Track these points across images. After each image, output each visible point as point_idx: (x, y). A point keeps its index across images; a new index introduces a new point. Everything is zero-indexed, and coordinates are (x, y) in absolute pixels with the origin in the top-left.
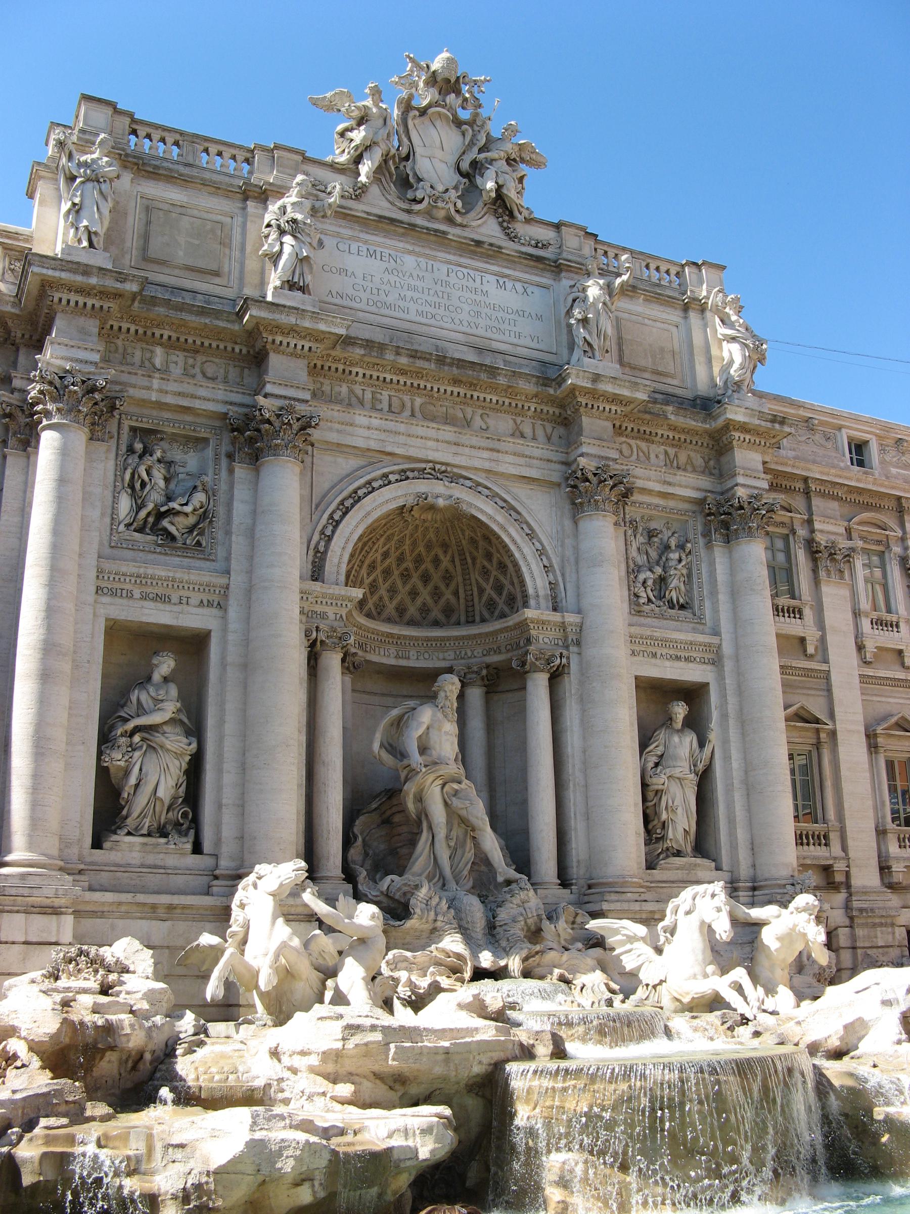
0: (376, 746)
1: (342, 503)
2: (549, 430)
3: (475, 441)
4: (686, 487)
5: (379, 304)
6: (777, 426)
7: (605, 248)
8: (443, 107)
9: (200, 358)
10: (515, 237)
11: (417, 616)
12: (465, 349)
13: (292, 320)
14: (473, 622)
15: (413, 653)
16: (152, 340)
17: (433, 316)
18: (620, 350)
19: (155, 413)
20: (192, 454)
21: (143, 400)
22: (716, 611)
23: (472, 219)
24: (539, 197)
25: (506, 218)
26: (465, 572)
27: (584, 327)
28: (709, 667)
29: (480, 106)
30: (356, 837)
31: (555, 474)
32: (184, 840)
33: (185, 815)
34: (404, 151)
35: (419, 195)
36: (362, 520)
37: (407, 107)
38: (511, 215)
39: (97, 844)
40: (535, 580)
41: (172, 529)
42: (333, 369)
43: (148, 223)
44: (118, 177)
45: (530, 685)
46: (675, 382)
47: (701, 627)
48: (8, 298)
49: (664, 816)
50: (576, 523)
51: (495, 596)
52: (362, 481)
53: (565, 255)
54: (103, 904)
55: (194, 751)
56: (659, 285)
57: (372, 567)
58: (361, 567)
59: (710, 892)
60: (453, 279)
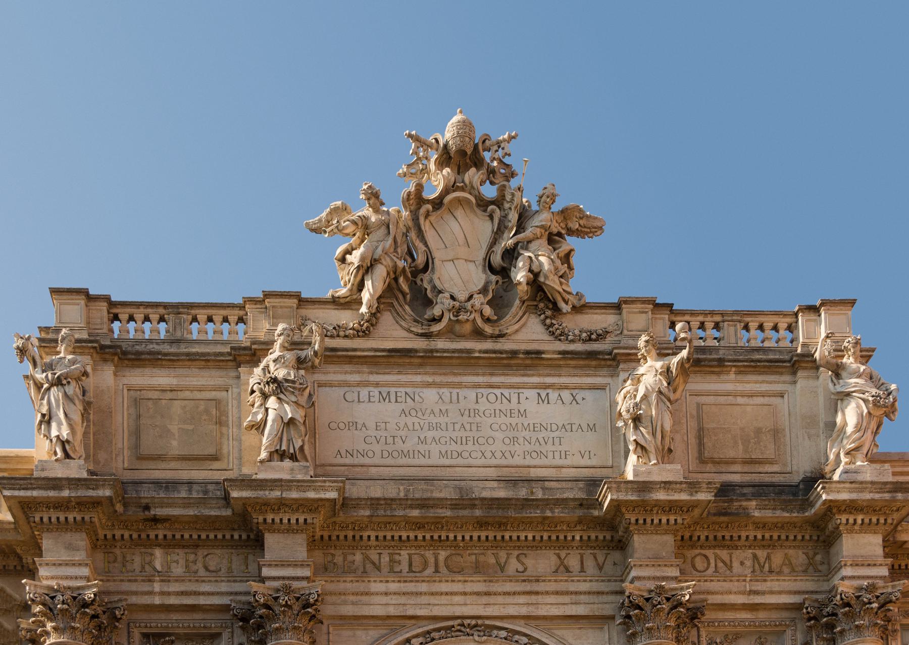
2: (601, 559)
3: (509, 587)
5: (395, 454)
9: (201, 552)
12: (495, 484)
17: (460, 455)
21: (148, 605)
23: (509, 323)
24: (594, 273)
25: (549, 313)
34: (420, 260)
38: (556, 309)
42: (342, 537)
43: (139, 417)
48: (8, 527)
60: (483, 406)
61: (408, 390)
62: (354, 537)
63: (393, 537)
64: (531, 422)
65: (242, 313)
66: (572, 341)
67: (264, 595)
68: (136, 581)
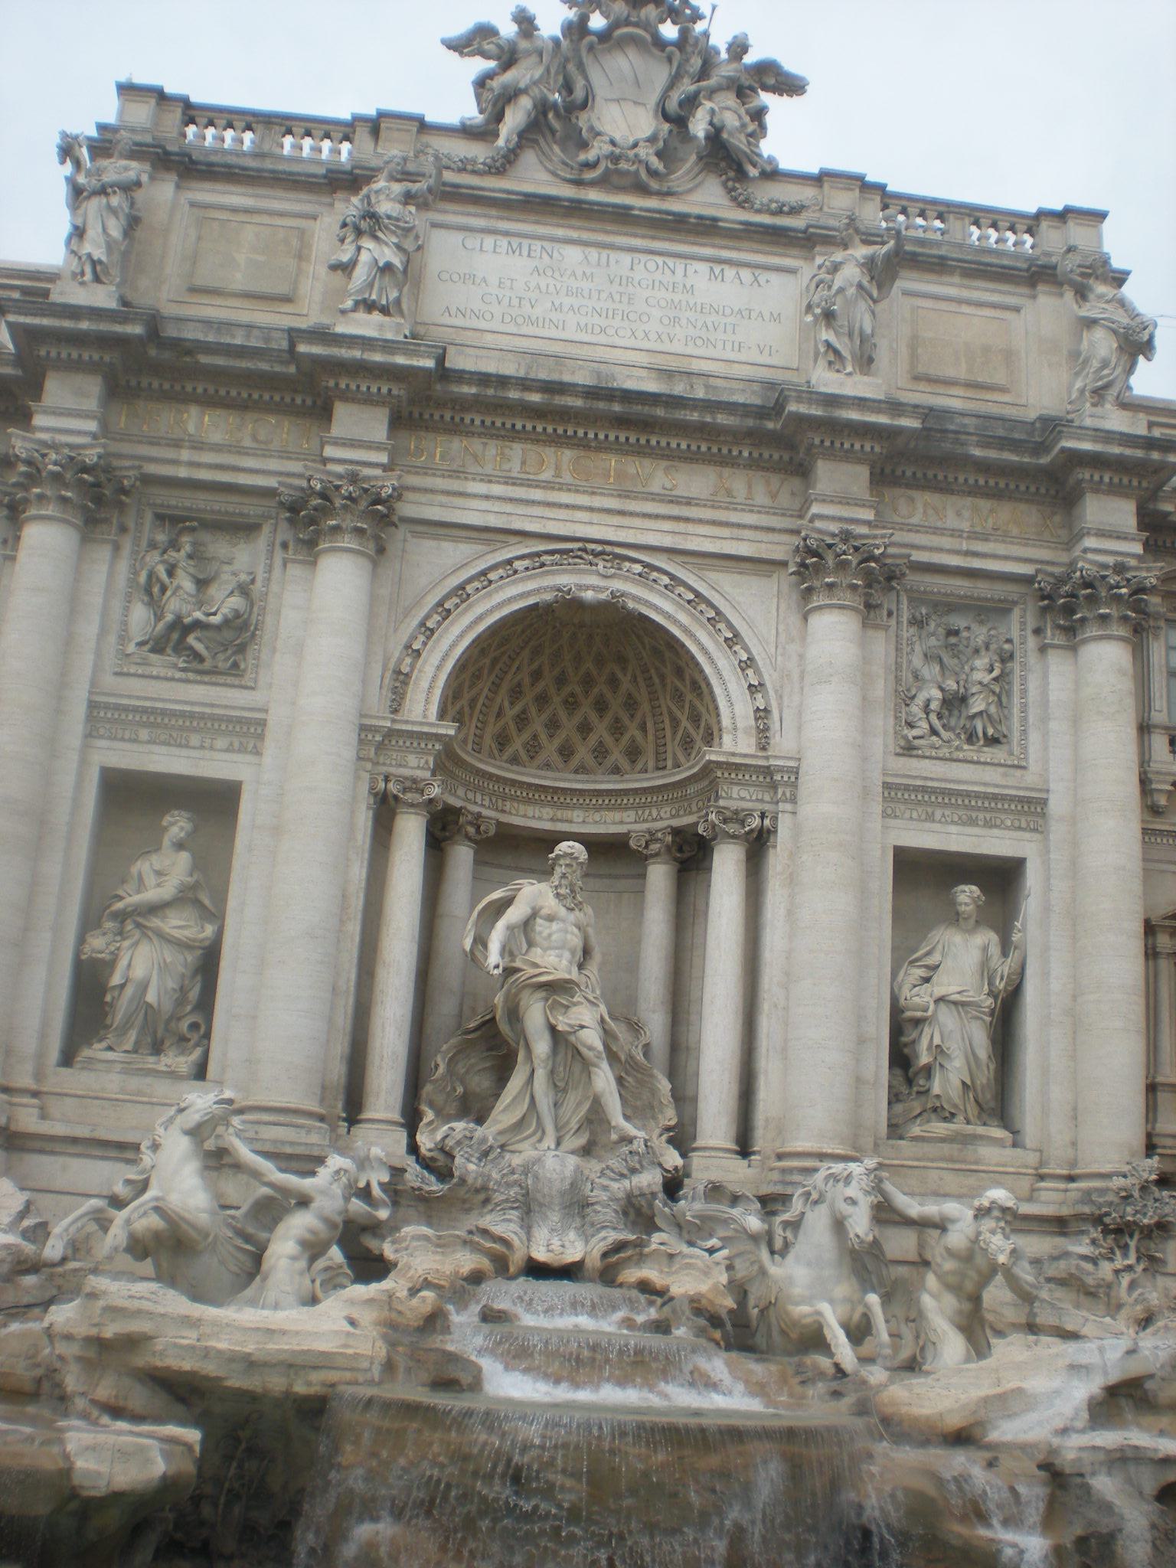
0: (468, 944)
1: (440, 604)
3: (650, 507)
4: (1006, 558)
5: (520, 320)
6: (1155, 455)
7: (904, 203)
8: (636, 25)
10: (746, 201)
11: (590, 761)
12: (644, 373)
13: (357, 354)
14: (665, 768)
15: (577, 815)
16: (185, 399)
17: (603, 330)
18: (914, 357)
19: (188, 494)
20: (242, 546)
22: (1046, 749)
24: (793, 138)
25: (732, 174)
26: (653, 697)
27: (829, 325)
28: (1027, 835)
29: (701, 17)
30: (437, 1066)
31: (778, 548)
32: (182, 1059)
33: (194, 1026)
35: (591, 155)
36: (470, 627)
37: (577, 29)
39: (67, 1059)
40: (733, 705)
41: (199, 647)
42: (437, 417)
43: (199, 238)
44: (138, 184)
45: (716, 857)
46: (1006, 398)
47: (1018, 773)
49: (924, 1059)
50: (805, 618)
51: (692, 731)
52: (472, 571)
53: (822, 222)
54: (53, 1138)
55: (207, 943)
56: (990, 252)
57: (516, 693)
58: (495, 693)
59: (845, 1174)
61: (546, 244)
62: (452, 418)
63: (503, 424)
64: (699, 302)
65: (348, 130)
66: (759, 211)
67: (322, 481)
68: (158, 444)
